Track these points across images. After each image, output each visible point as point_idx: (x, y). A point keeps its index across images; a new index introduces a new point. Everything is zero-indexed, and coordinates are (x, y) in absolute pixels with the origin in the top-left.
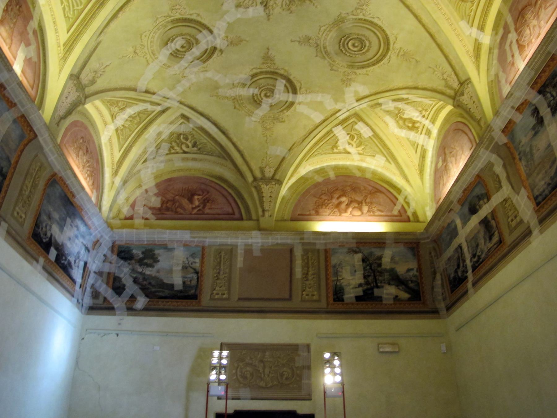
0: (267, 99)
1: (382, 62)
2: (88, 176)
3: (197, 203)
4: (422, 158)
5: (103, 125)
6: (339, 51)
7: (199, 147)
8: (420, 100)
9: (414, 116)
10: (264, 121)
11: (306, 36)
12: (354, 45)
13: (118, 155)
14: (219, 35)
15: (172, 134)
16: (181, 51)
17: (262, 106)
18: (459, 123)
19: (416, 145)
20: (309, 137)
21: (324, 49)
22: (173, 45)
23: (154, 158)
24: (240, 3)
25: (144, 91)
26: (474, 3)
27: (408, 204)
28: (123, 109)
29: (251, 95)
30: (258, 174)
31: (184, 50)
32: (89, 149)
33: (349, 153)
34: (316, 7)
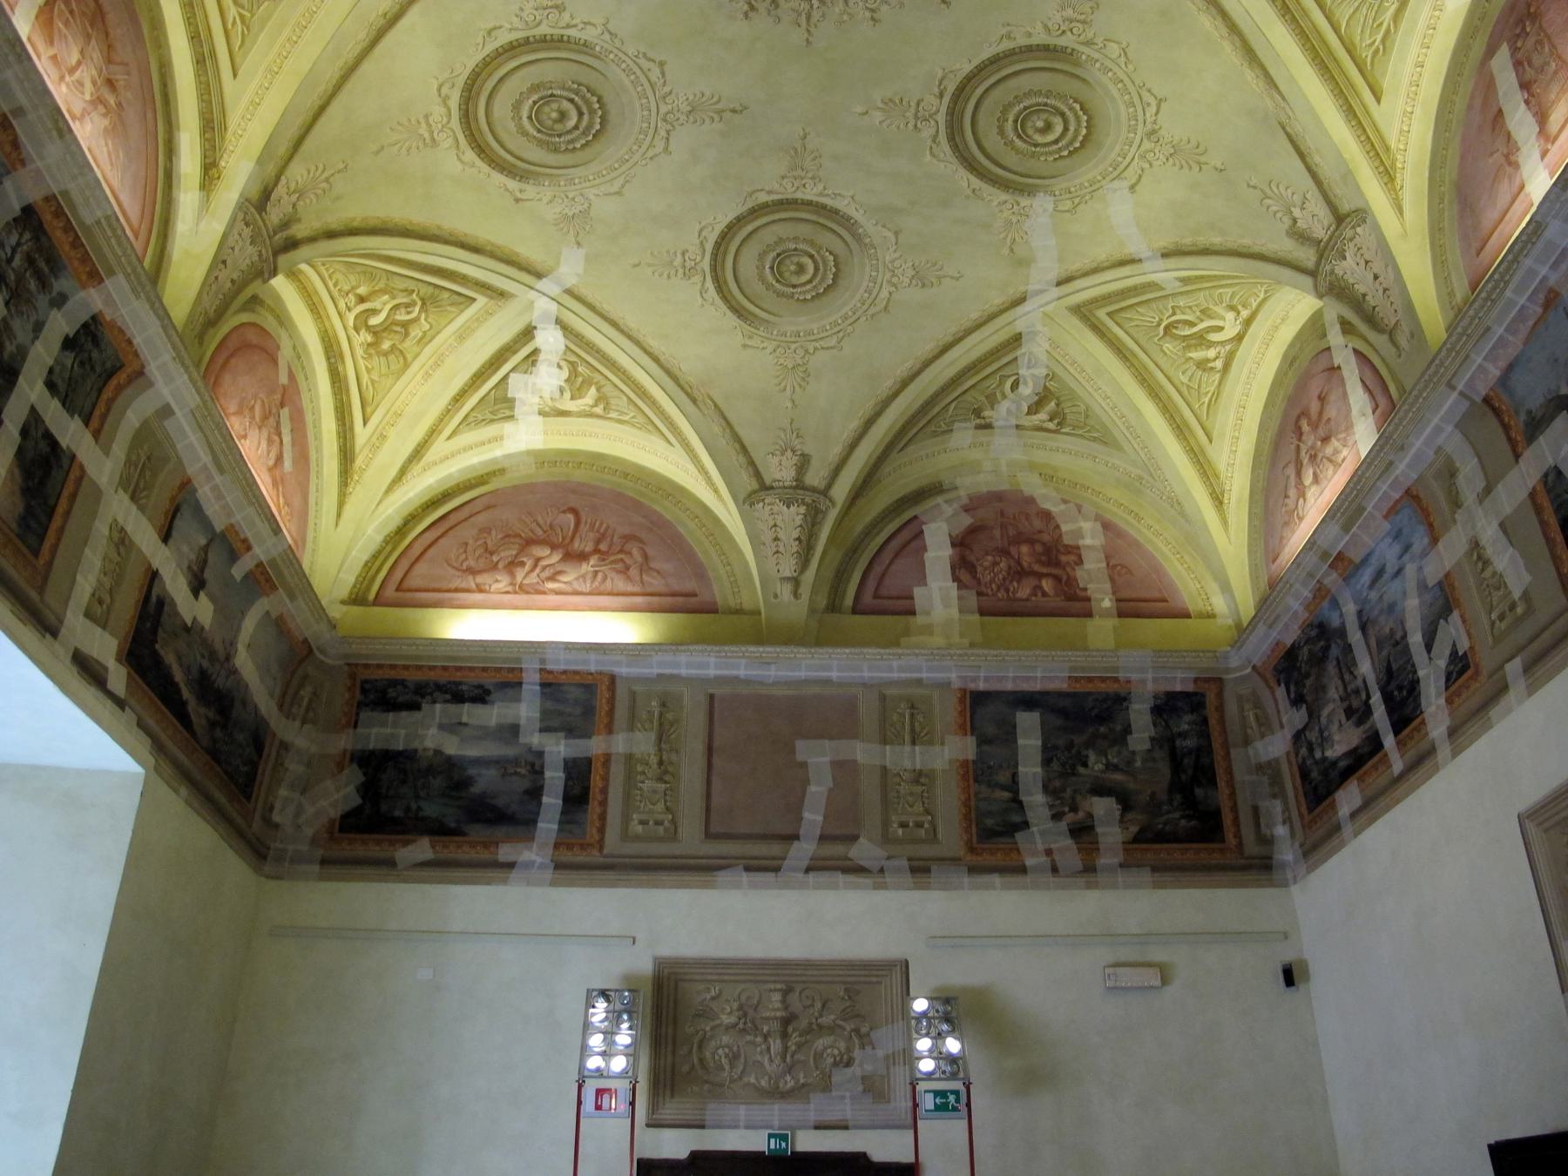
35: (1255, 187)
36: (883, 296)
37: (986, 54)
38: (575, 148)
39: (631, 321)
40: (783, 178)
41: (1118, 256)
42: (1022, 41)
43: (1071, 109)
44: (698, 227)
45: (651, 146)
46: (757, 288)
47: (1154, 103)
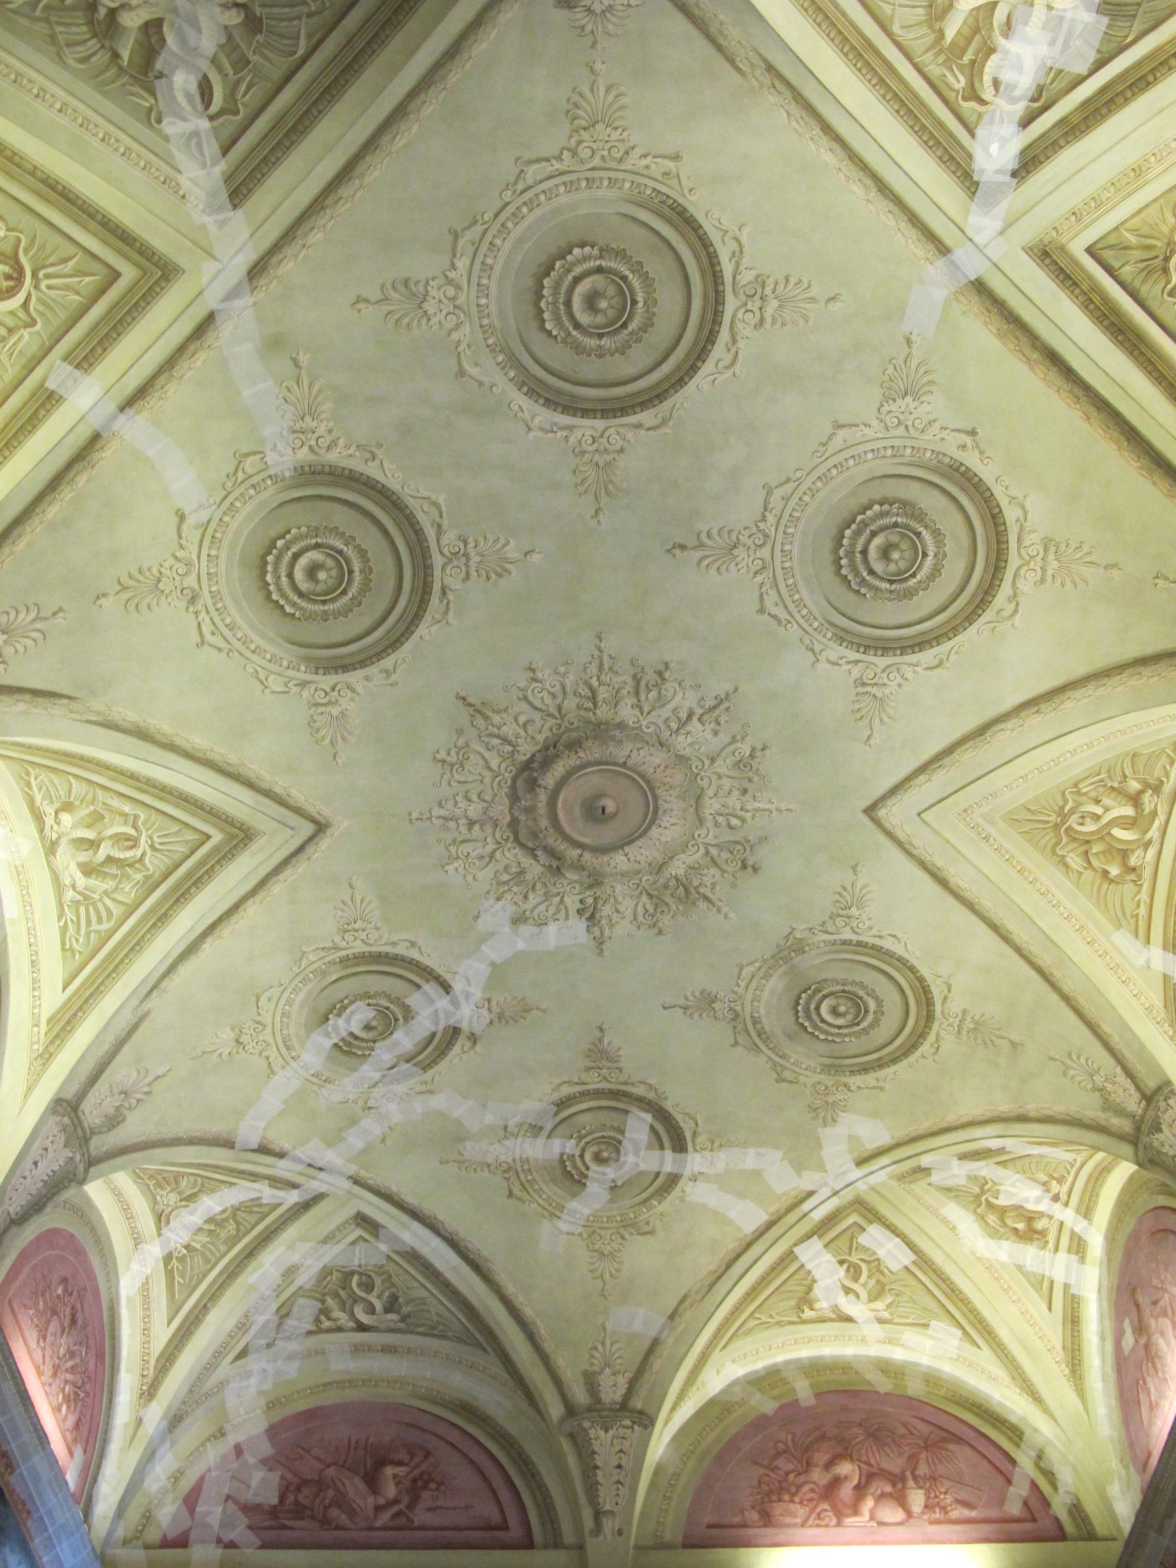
0: (601, 1169)
1: (918, 1053)
2: (67, 1399)
3: (391, 1491)
4: (1069, 1325)
5: (131, 1244)
6: (797, 1028)
7: (405, 1310)
8: (1036, 1150)
9: (1027, 1200)
10: (594, 1232)
11: (702, 992)
12: (834, 1012)
13: (162, 1335)
14: (468, 996)
15: (326, 1272)
16: (362, 1040)
17: (588, 1190)
18: (1160, 1212)
19: (1046, 1284)
20: (726, 1275)
21: (754, 1024)
22: (341, 1022)
23: (269, 1346)
24: (524, 912)
25: (256, 1147)
26: (1141, 885)
27: (1050, 1475)
28: (191, 1198)
29: (557, 1157)
30: (580, 1396)
31: (371, 1035)
32: (79, 1316)
33: (849, 1319)
34: (726, 916)
35: (54, 614)
36: (463, 259)
37: (408, 646)
38: (881, 505)
39: (857, 192)
40: (621, 451)
41: (152, 401)
42: (373, 670)
43: (294, 605)
44: (737, 368)
45: (786, 499)
46: (659, 267)
47: (208, 637)
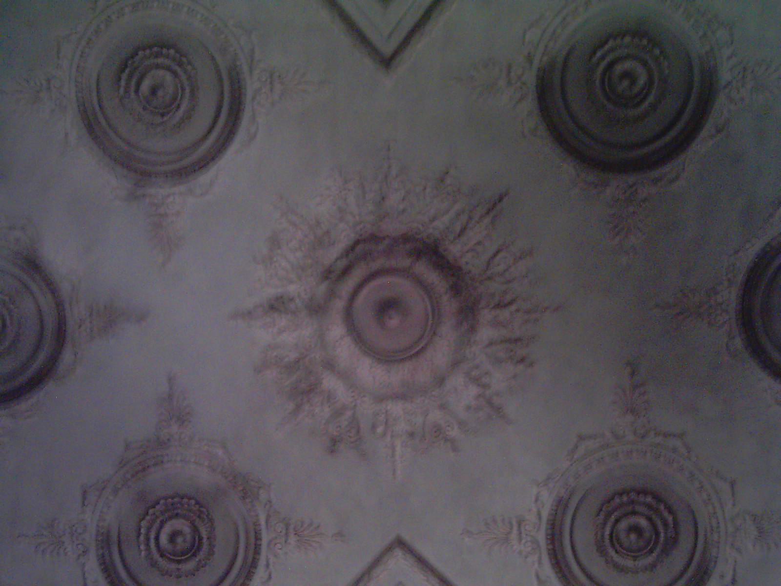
43: (603, 58)
